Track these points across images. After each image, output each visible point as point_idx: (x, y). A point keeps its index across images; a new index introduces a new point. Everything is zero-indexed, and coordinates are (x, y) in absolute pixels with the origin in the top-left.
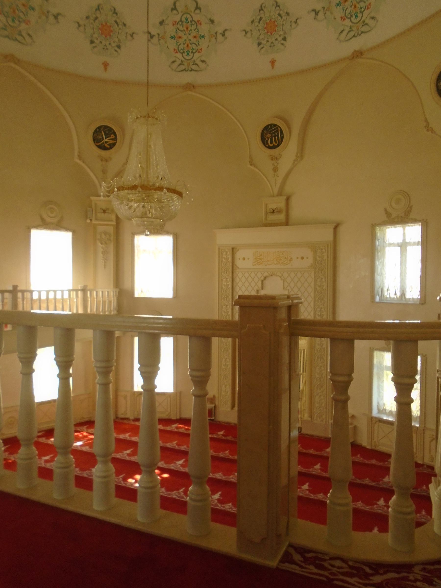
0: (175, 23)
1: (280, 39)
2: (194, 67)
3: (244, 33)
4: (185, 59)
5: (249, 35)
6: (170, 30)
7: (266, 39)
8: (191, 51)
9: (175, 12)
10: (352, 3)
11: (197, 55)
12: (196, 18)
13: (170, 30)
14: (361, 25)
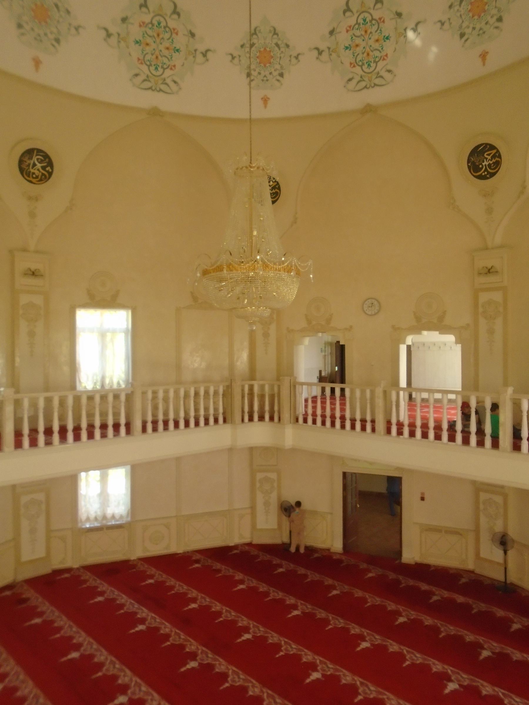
0: (142, 24)
1: (275, 73)
2: (163, 87)
3: (230, 57)
4: (152, 74)
5: (236, 61)
6: (136, 32)
7: (257, 70)
8: (161, 66)
9: (144, 9)
10: (364, 49)
11: (168, 72)
12: (172, 24)
13: (136, 32)
14: (374, 77)
